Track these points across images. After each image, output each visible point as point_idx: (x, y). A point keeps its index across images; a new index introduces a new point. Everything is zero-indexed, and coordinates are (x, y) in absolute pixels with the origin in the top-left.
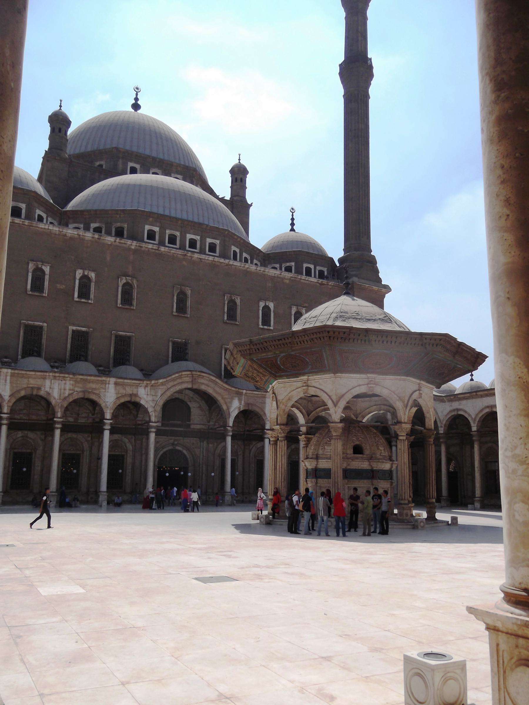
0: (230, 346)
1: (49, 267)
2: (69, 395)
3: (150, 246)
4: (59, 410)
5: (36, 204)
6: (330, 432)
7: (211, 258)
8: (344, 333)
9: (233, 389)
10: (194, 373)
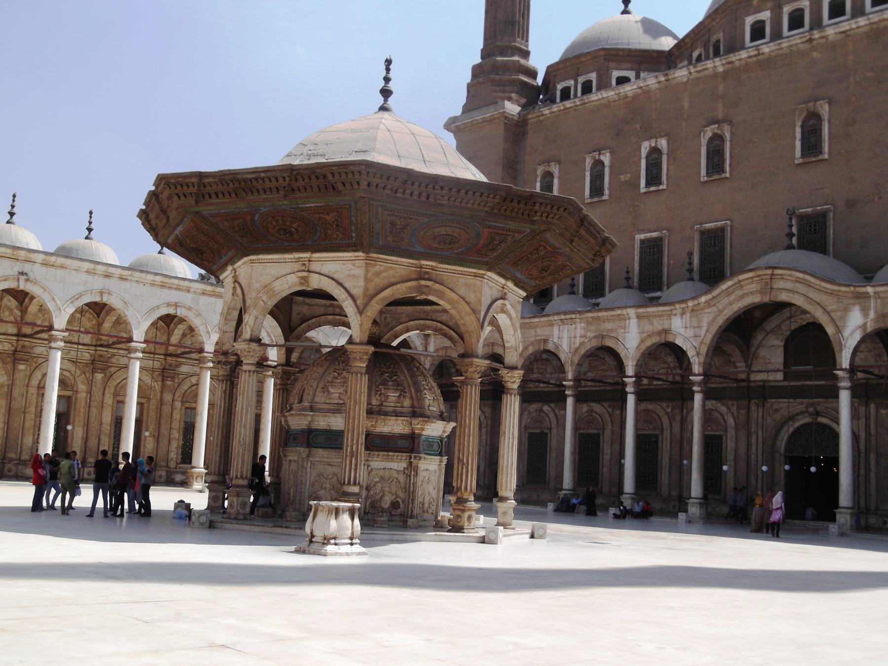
1: (608, 154)
2: (582, 344)
3: (767, 48)
5: (612, 65)
9: (843, 289)
10: (760, 273)
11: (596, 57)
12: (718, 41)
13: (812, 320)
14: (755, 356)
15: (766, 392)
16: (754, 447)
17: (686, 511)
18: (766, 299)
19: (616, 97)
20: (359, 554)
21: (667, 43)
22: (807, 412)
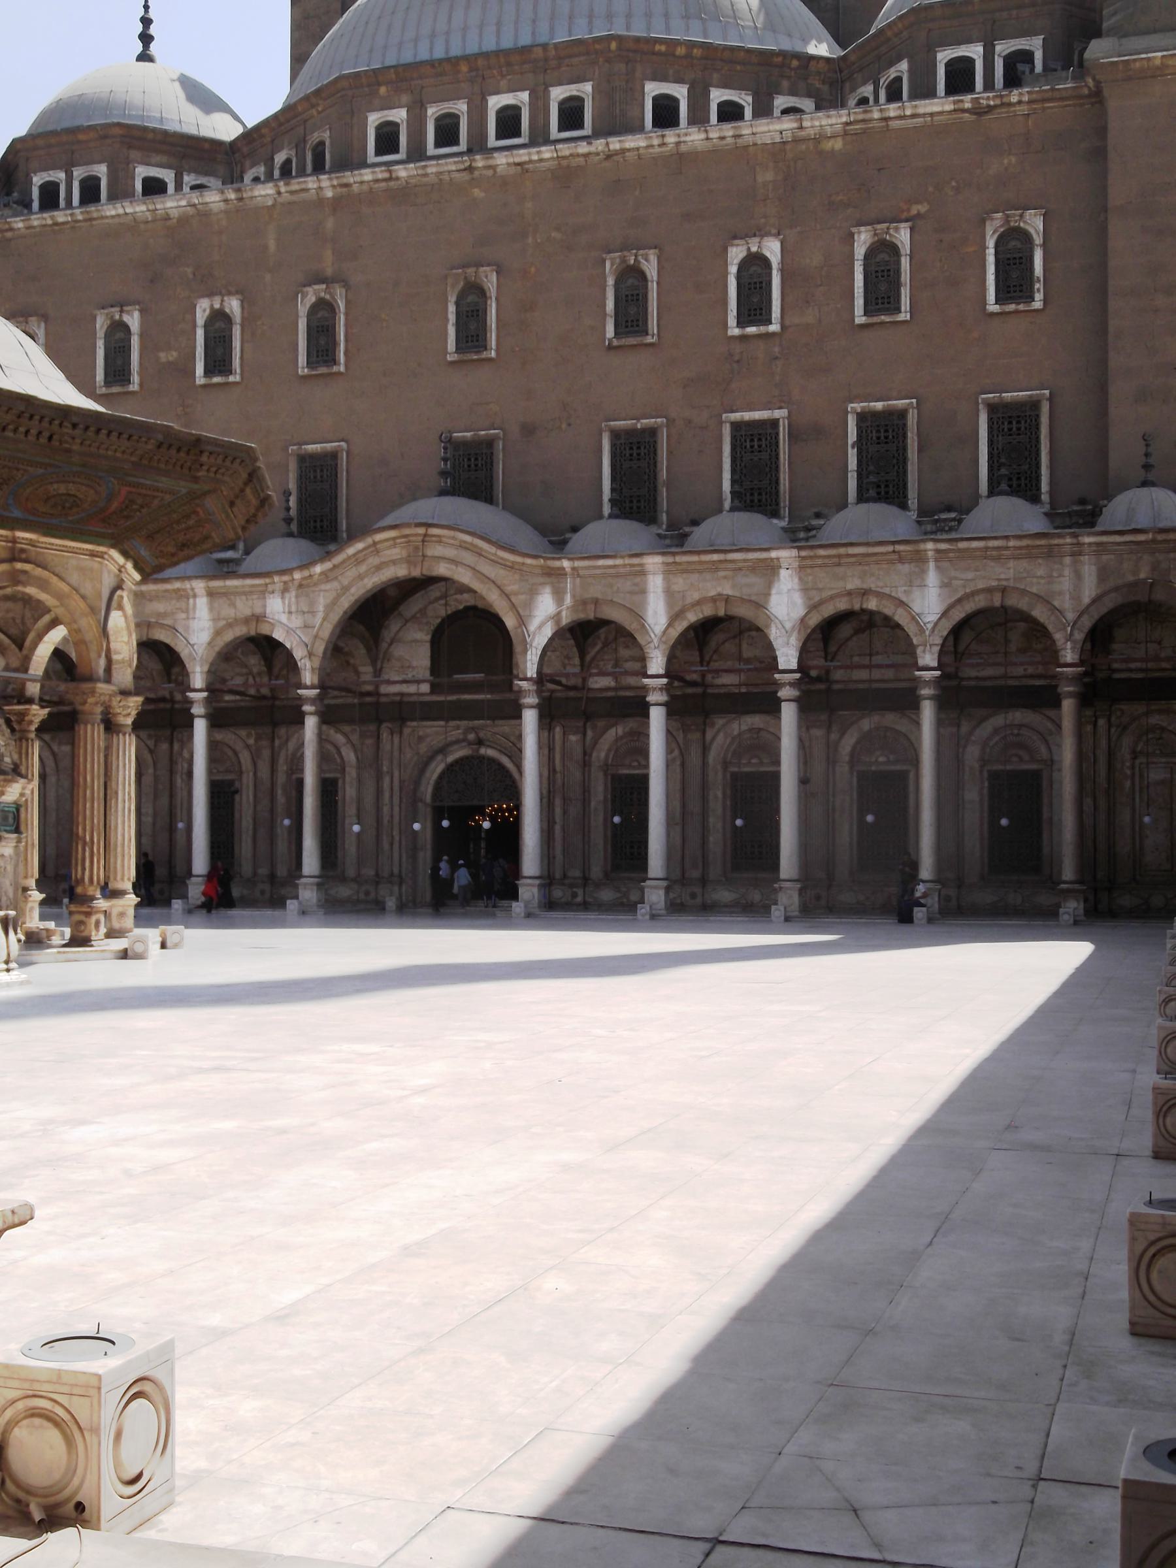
1: (136, 314)
5: (134, 154)
9: (529, 561)
10: (407, 531)
11: (105, 137)
12: (322, 143)
13: (471, 603)
14: (387, 657)
15: (402, 712)
16: (387, 795)
17: (297, 897)
18: (416, 573)
19: (149, 216)
20: (22, 983)
21: (225, 130)
22: (464, 740)
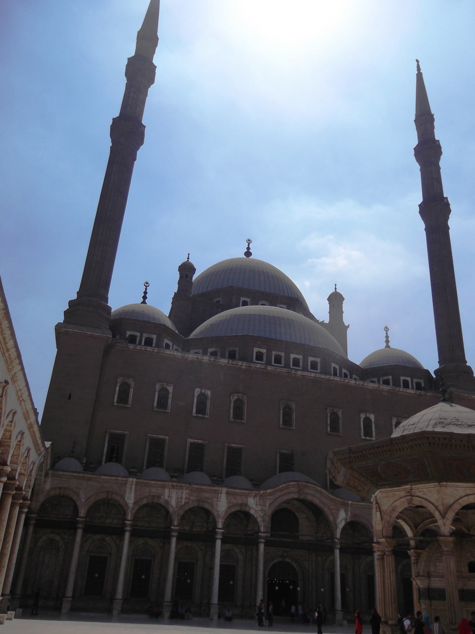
0: (331, 455)
1: (172, 387)
4: (176, 519)
6: (441, 546)
7: (313, 375)
8: (445, 439)
9: (339, 499)
10: (300, 483)
